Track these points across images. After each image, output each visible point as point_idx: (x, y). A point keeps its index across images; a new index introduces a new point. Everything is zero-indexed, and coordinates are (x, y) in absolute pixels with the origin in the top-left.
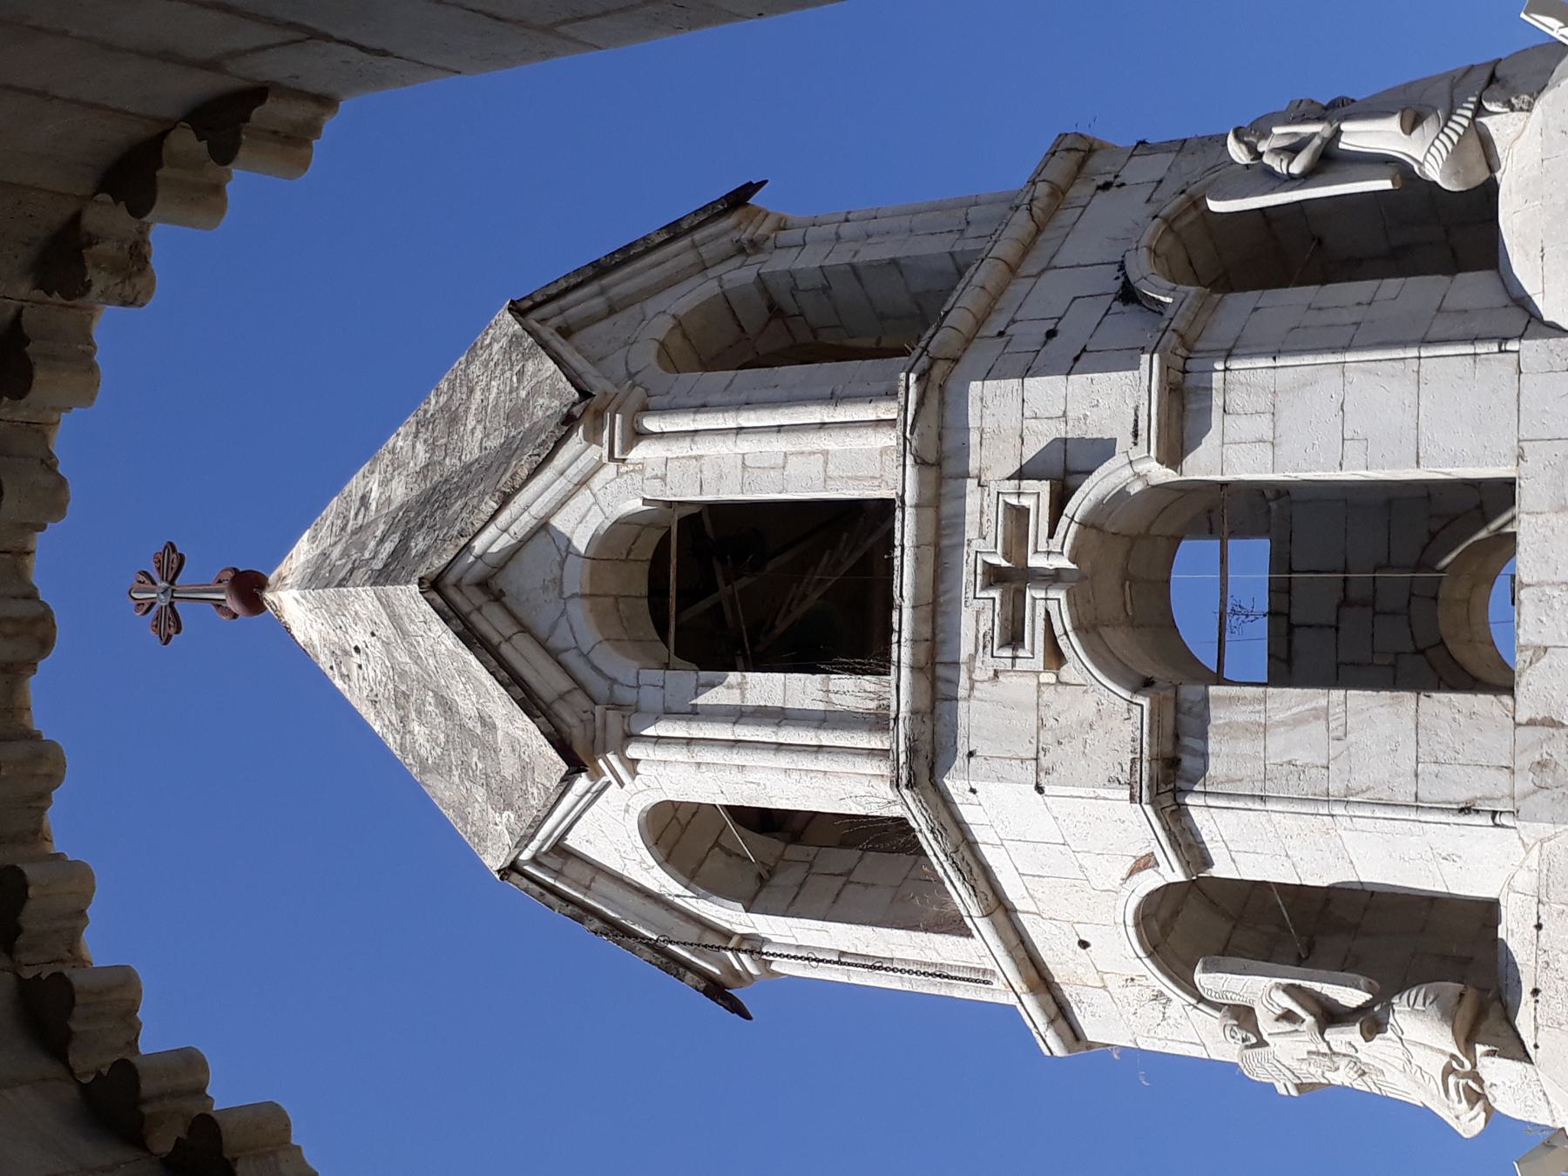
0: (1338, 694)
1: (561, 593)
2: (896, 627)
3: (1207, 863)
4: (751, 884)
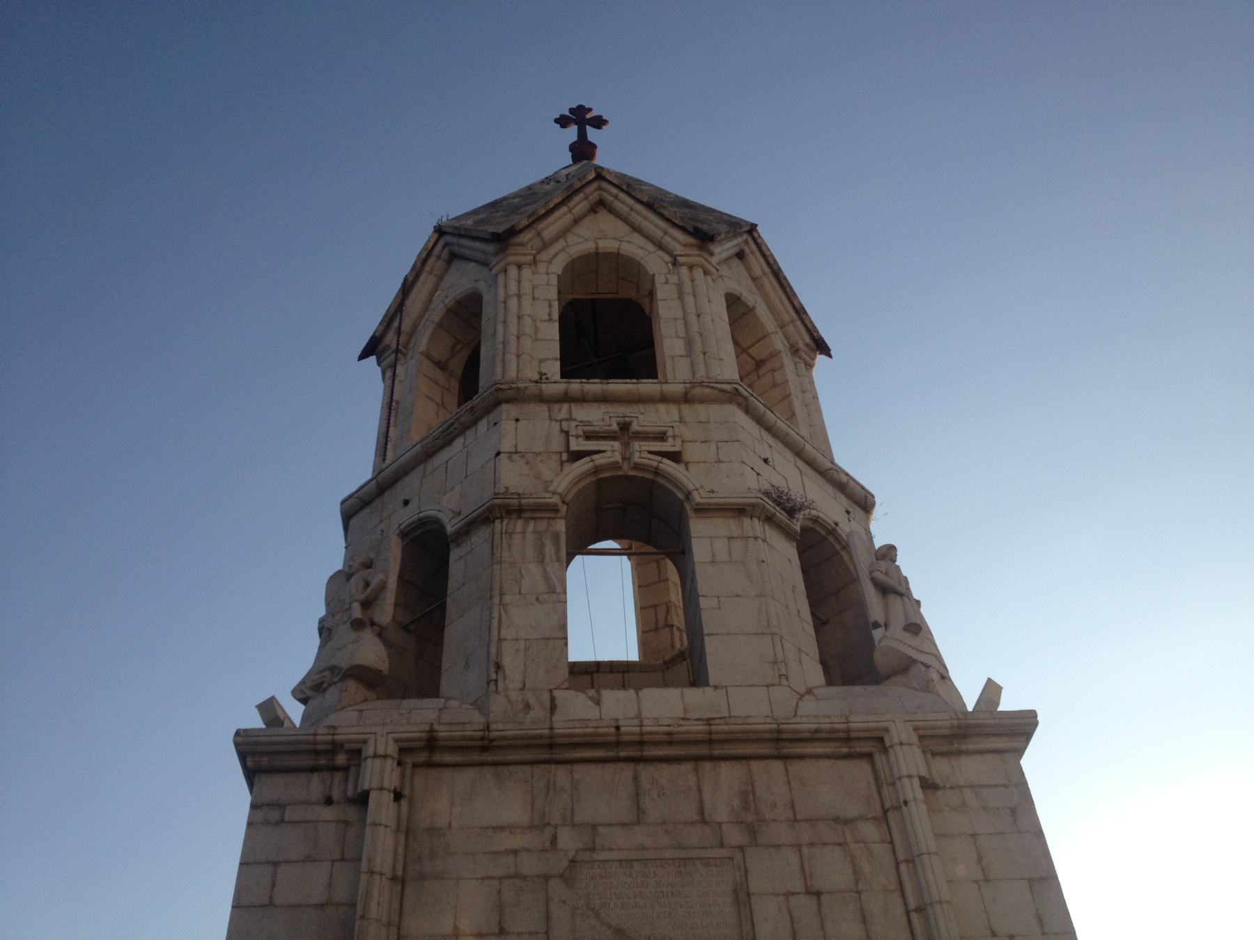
3: (458, 546)
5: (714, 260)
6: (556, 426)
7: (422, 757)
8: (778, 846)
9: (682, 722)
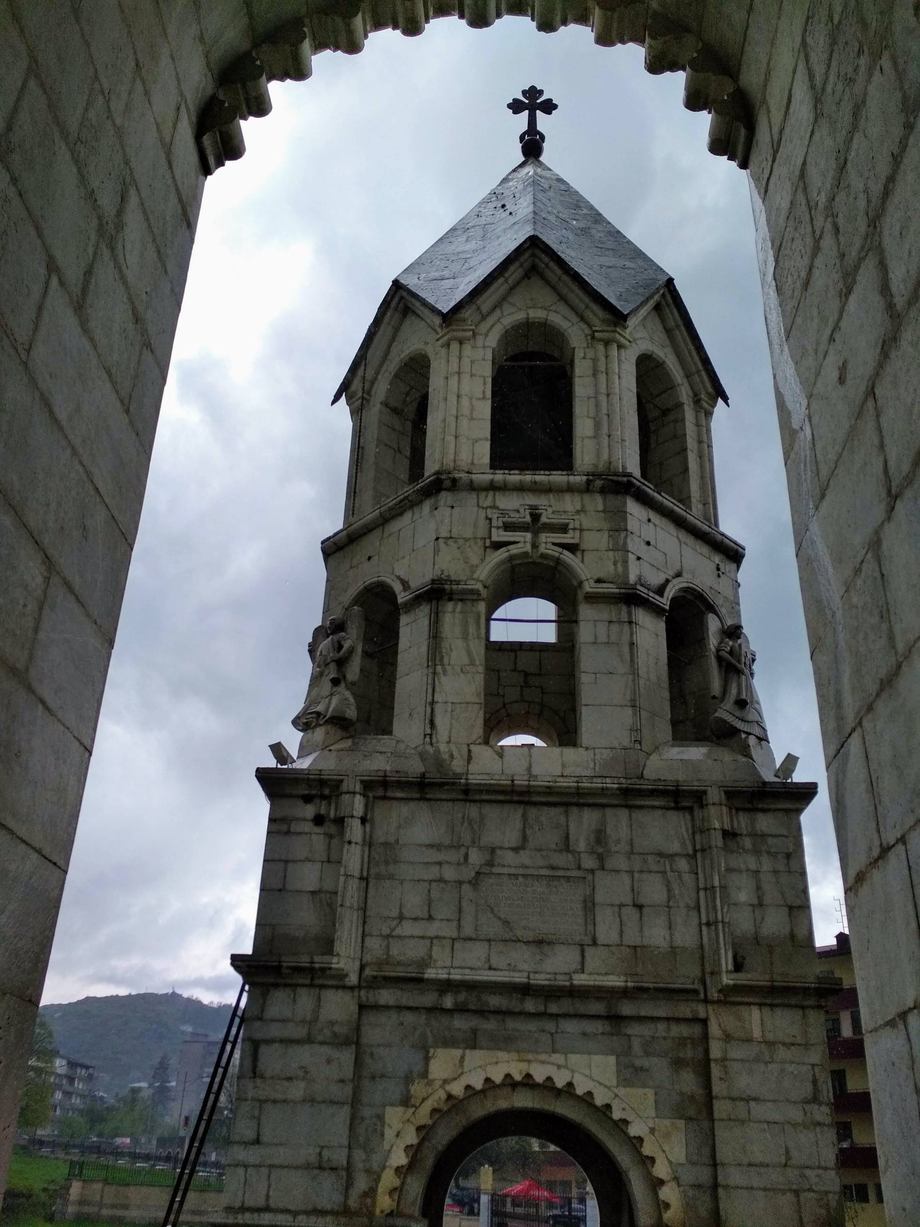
0: (481, 669)
1: (529, 308)
2: (512, 472)
3: (406, 613)
4: (393, 404)
5: (628, 331)
6: (482, 514)
7: (380, 792)
8: (617, 871)
9: (559, 779)
